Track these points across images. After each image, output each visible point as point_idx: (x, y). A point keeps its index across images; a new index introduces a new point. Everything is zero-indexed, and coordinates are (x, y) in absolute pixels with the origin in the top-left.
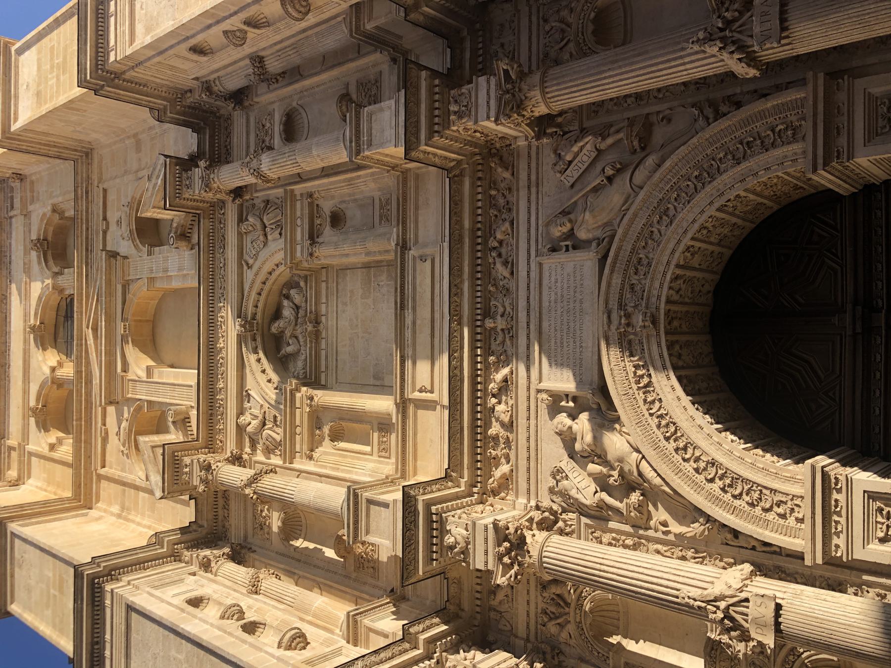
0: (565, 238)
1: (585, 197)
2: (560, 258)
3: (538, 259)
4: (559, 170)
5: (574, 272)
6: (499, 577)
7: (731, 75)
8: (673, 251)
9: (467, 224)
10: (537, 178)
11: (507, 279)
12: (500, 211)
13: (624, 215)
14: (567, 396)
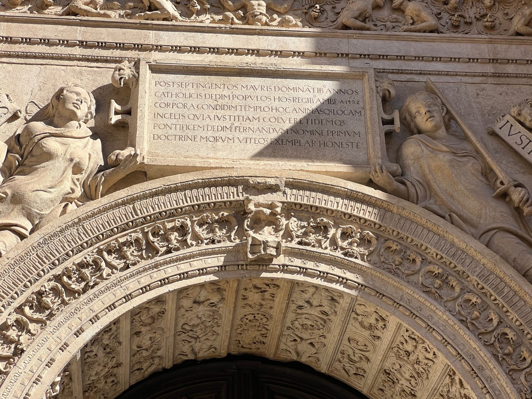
0: (405, 119)
1: (475, 154)
2: (371, 109)
3: (372, 71)
4: (523, 112)
5: (347, 133)
10: (508, 76)
11: (334, 18)
12: (456, 9)
13: (443, 217)
14: (129, 113)
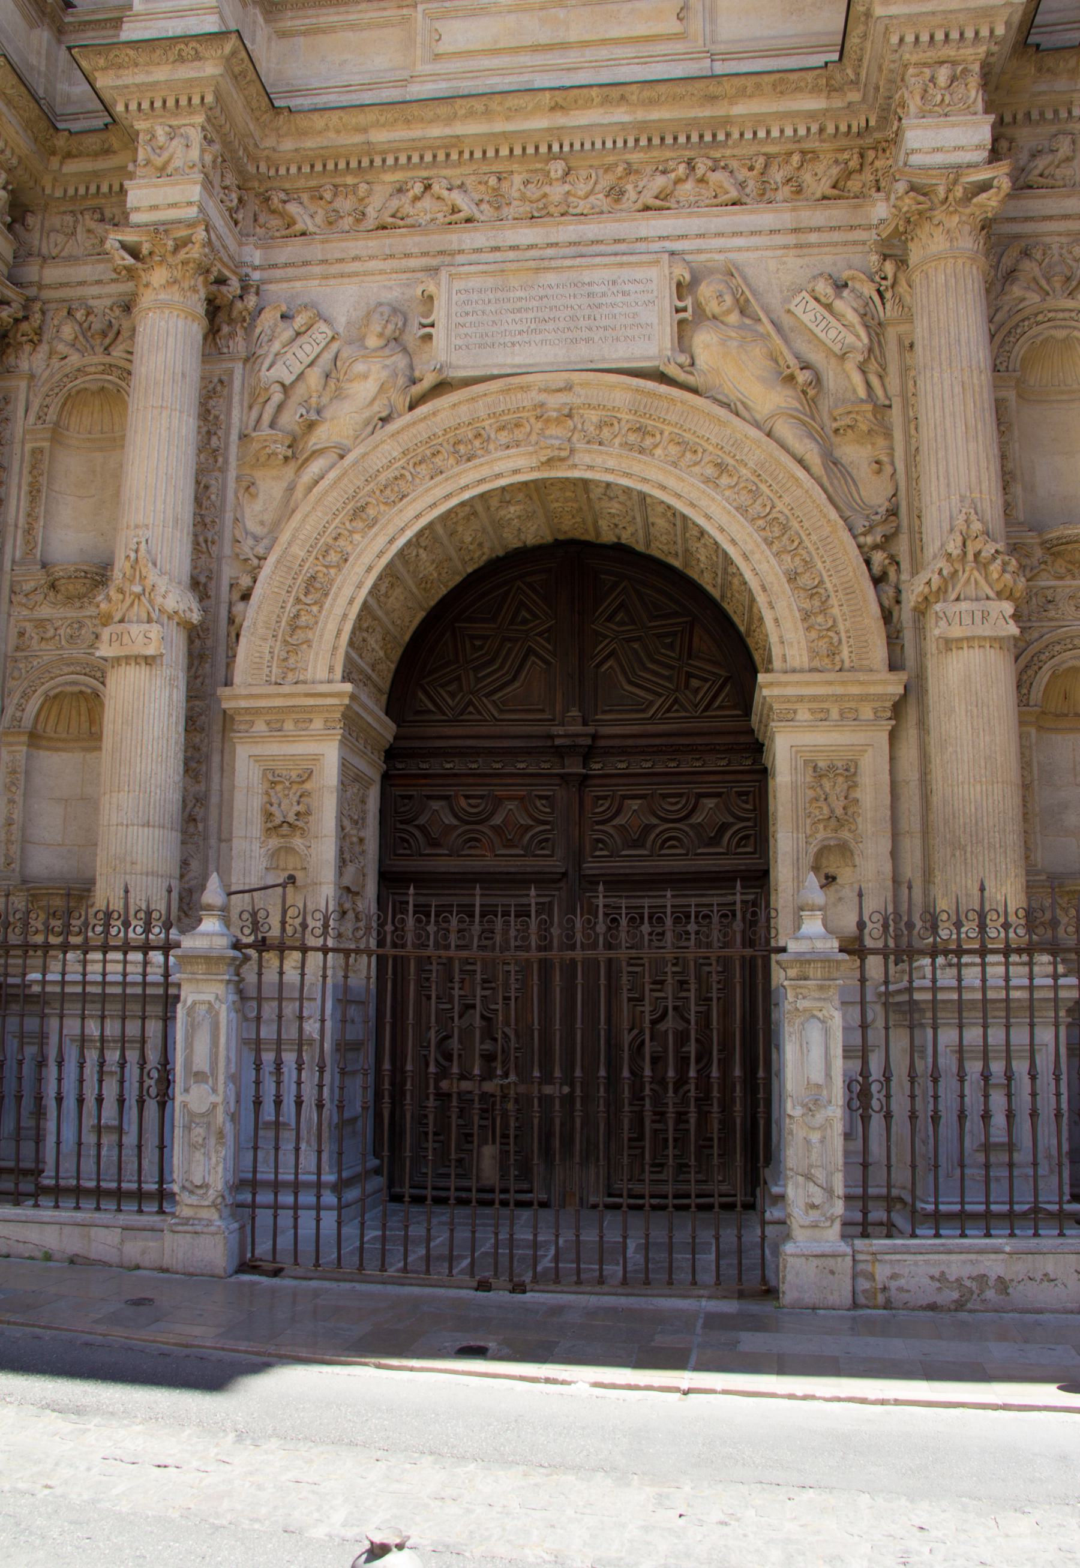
6: (120, 238)
7: (916, 569)
8: (663, 488)
9: (740, 109)
10: (809, 246)
